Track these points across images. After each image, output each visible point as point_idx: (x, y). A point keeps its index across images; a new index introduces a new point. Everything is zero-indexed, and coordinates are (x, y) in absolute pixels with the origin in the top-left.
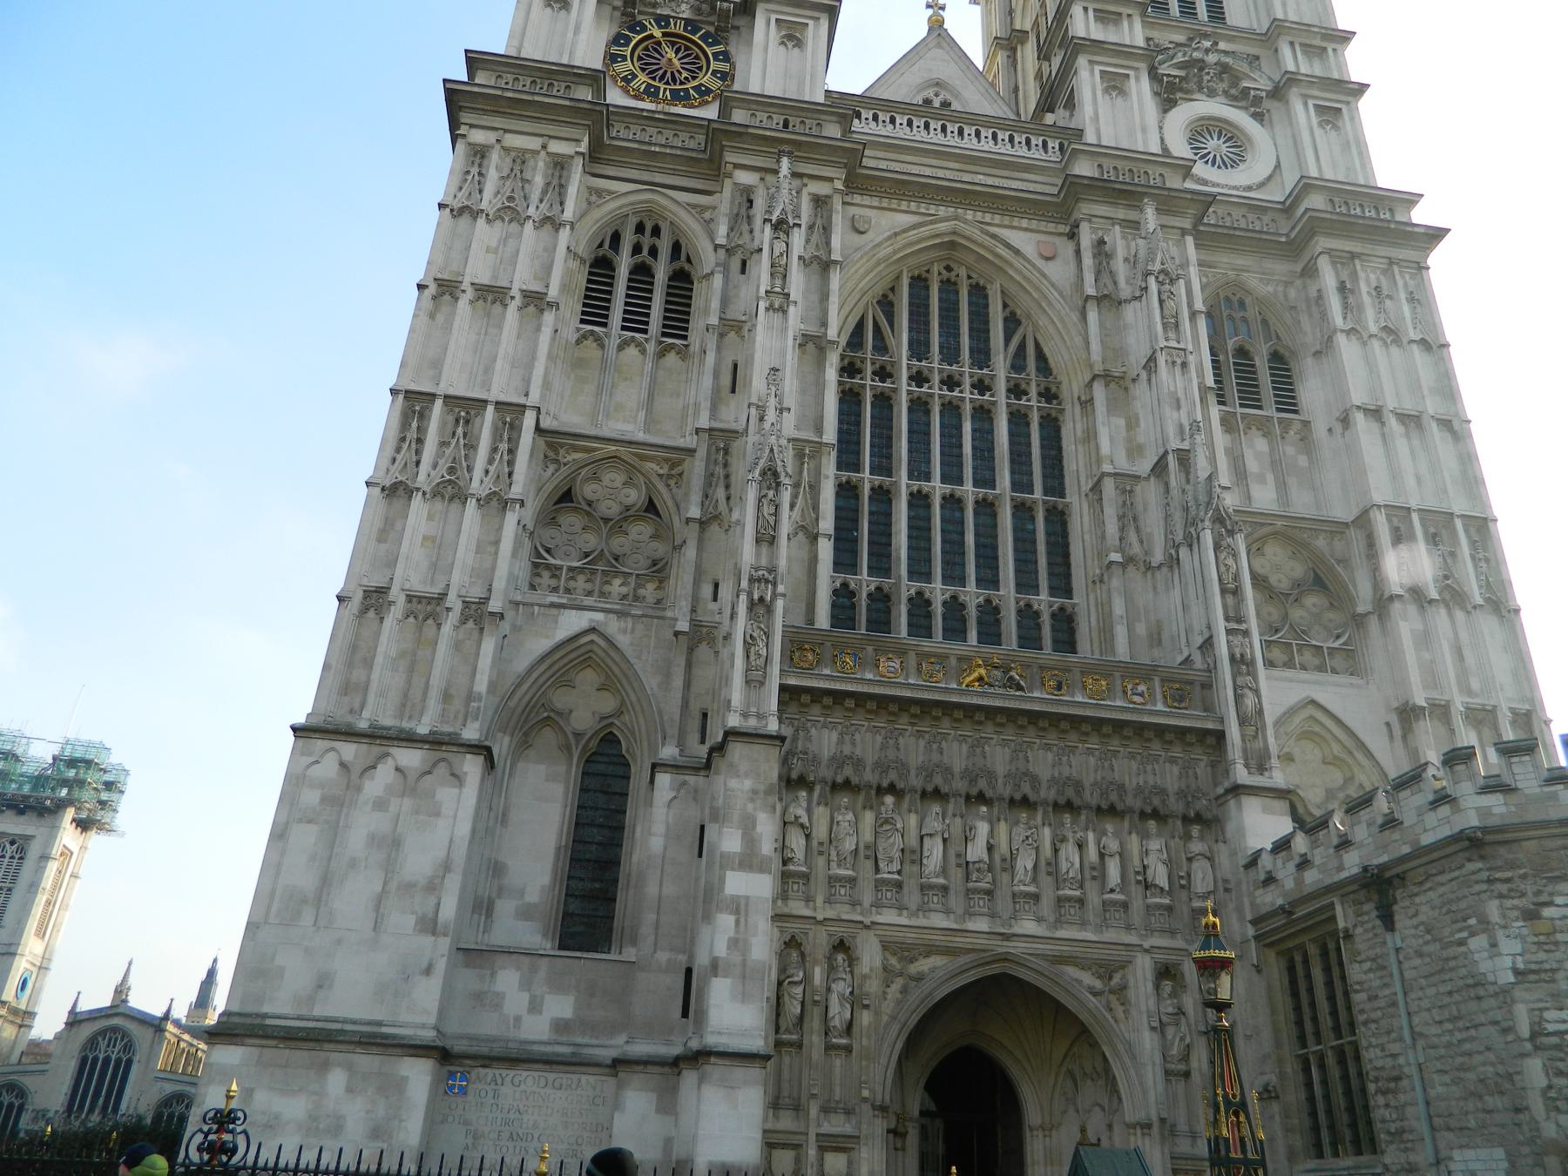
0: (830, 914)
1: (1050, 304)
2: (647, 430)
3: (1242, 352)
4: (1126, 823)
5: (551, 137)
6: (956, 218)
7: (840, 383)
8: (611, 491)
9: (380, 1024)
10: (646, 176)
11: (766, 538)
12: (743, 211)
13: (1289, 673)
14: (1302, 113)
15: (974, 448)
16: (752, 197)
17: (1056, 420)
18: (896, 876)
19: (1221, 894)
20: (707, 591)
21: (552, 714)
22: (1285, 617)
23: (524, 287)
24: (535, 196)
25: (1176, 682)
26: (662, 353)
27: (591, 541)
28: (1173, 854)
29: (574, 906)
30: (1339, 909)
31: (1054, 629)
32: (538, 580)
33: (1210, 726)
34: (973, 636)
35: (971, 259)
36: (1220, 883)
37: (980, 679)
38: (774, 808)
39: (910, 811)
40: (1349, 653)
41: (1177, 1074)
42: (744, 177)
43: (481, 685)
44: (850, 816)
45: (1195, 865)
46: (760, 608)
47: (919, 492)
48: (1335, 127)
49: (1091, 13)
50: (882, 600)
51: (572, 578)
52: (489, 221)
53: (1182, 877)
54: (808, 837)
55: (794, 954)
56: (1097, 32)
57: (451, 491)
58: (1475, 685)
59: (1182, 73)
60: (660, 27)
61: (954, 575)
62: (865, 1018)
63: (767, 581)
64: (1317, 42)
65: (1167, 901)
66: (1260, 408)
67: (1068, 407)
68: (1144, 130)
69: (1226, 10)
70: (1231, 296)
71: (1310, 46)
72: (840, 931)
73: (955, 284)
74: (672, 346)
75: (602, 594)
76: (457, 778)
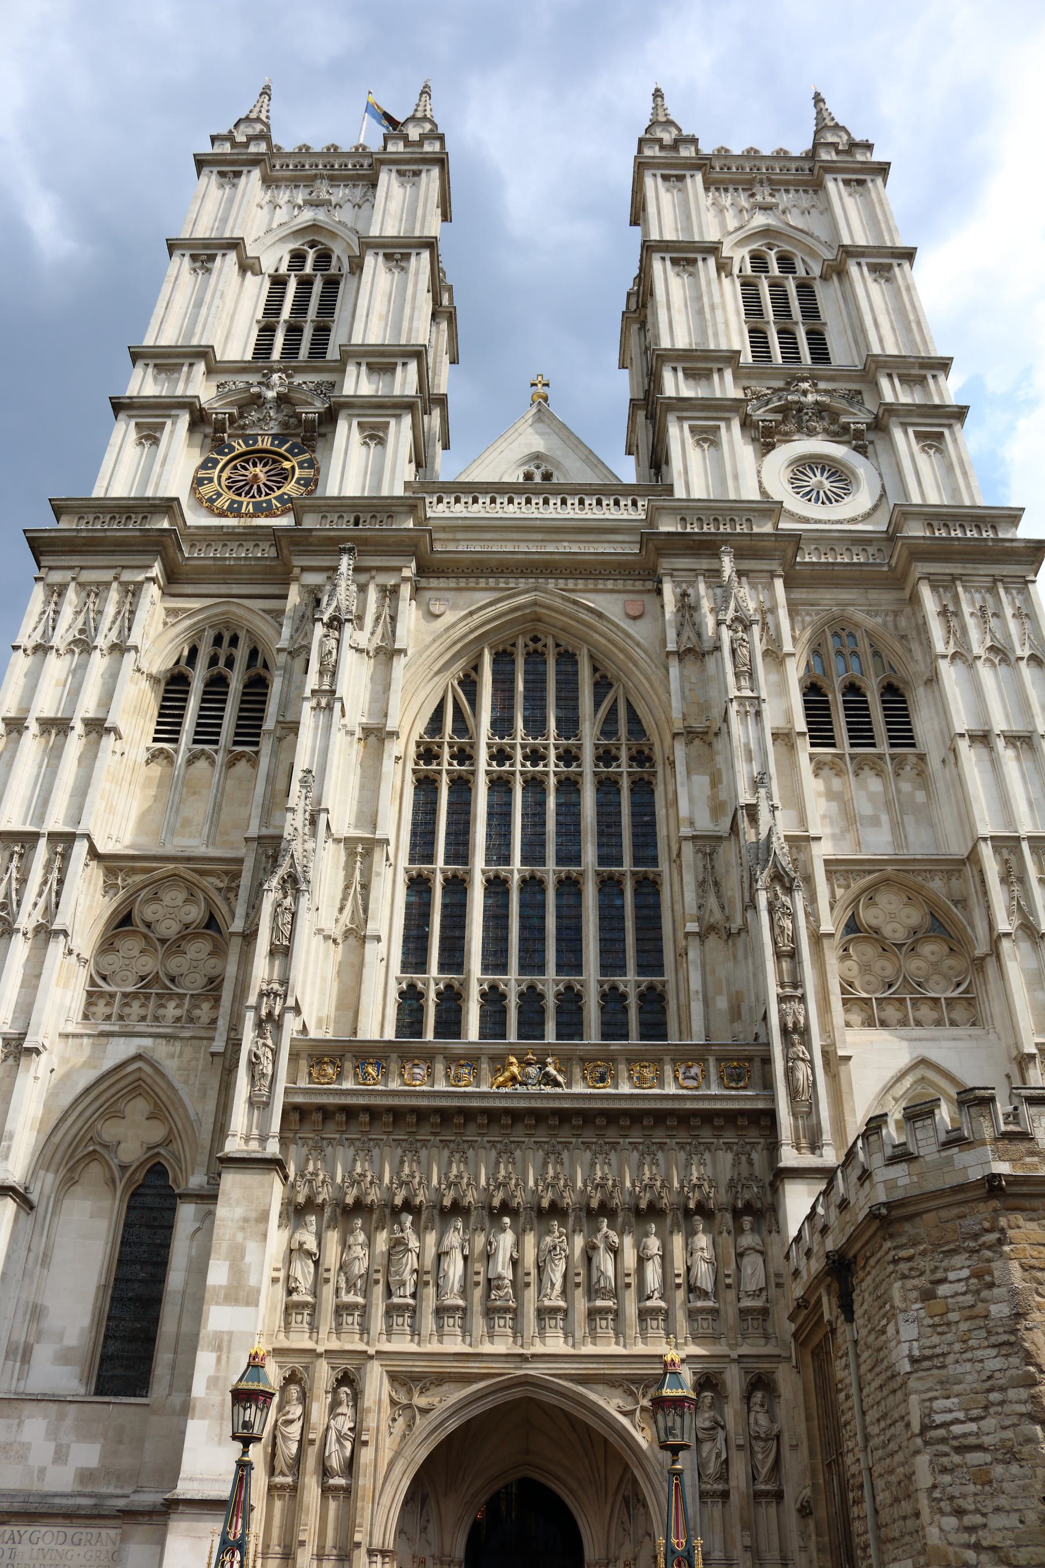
0: (334, 1344)
1: (636, 665)
2: (210, 842)
3: (852, 689)
4: (669, 1221)
5: (123, 567)
7: (414, 771)
8: (171, 910)
10: (224, 589)
12: (309, 613)
14: (903, 440)
15: (558, 824)
16: (320, 596)
17: (650, 783)
18: (411, 1301)
19: (773, 1290)
21: (98, 1148)
22: (899, 970)
23: (88, 715)
25: (733, 1060)
26: (233, 760)
27: (148, 964)
28: (719, 1250)
29: (114, 1347)
30: (825, 1300)
31: (641, 1009)
32: (93, 1009)
33: (761, 1105)
34: (550, 1028)
35: (555, 631)
36: (773, 1281)
37: (513, 1079)
38: (265, 1236)
39: (426, 1228)
40: (970, 1001)
41: (714, 1494)
42: (312, 579)
44: (361, 1237)
45: (746, 1260)
47: (497, 877)
48: (939, 450)
49: (680, 374)
51: (127, 1004)
52: (59, 655)
53: (728, 1276)
54: (316, 1263)
55: (294, 1390)
56: (687, 390)
59: (779, 417)
60: (247, 445)
61: (532, 962)
62: (366, 1455)
63: (276, 995)
65: (710, 1304)
66: (873, 745)
67: (659, 769)
68: (736, 477)
69: (830, 350)
70: (840, 632)
71: (909, 375)
72: (344, 1363)
73: (543, 654)
74: (242, 755)
75: (156, 1018)
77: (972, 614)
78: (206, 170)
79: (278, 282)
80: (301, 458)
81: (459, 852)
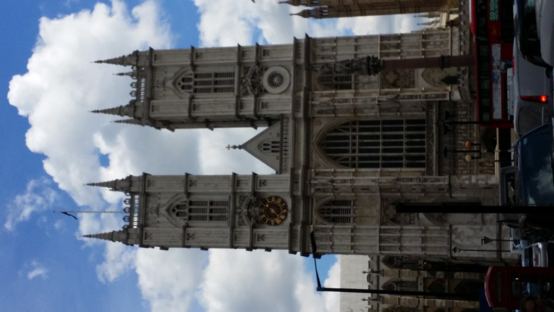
0: (476, 166)
3: (336, 79)
6: (313, 144)
9: (497, 234)
11: (411, 180)
13: (416, 78)
14: (266, 59)
20: (414, 191)
24: (326, 234)
26: (355, 205)
42: (313, 190)
43: (439, 228)
44: (459, 164)
46: (425, 180)
49: (241, 110)
50: (408, 158)
52: (333, 242)
55: (483, 172)
57: (400, 239)
58: (417, 44)
60: (263, 214)
64: (241, 52)
68: (279, 99)
74: (353, 203)
76: (456, 229)
77: (323, 52)
78: (144, 243)
79: (190, 218)
80: (268, 200)
81: (377, 158)
